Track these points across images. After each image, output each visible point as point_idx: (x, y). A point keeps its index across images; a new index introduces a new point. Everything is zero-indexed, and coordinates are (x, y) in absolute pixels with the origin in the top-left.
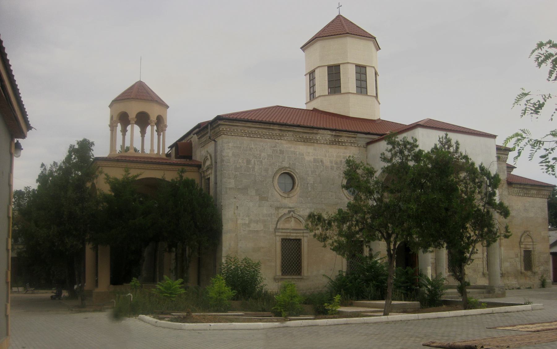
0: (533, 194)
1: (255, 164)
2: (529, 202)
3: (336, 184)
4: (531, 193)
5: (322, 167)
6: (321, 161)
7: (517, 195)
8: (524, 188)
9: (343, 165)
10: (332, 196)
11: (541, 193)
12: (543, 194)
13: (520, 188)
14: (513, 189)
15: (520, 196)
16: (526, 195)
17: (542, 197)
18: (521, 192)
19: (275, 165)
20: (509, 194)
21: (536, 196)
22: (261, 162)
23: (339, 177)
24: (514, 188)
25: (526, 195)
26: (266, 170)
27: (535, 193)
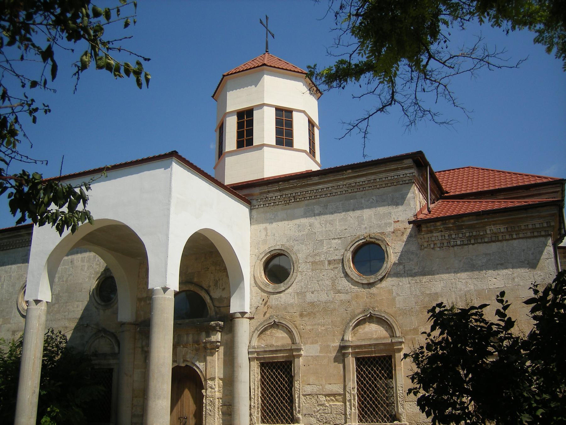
0: (496, 233)
1: (4, 280)
2: (486, 254)
3: (84, 289)
4: (488, 232)
5: (71, 269)
6: (71, 262)
7: (446, 244)
8: (460, 228)
9: (96, 260)
10: (77, 307)
11: (523, 227)
12: (530, 227)
13: (448, 229)
14: (429, 235)
15: (457, 245)
16: (472, 241)
17: (529, 234)
18: (453, 236)
19: (23, 277)
20: (421, 247)
21: (507, 237)
22: (10, 276)
23: (90, 278)
24: (431, 232)
25: (472, 241)
26: (13, 285)
27: (502, 230)
